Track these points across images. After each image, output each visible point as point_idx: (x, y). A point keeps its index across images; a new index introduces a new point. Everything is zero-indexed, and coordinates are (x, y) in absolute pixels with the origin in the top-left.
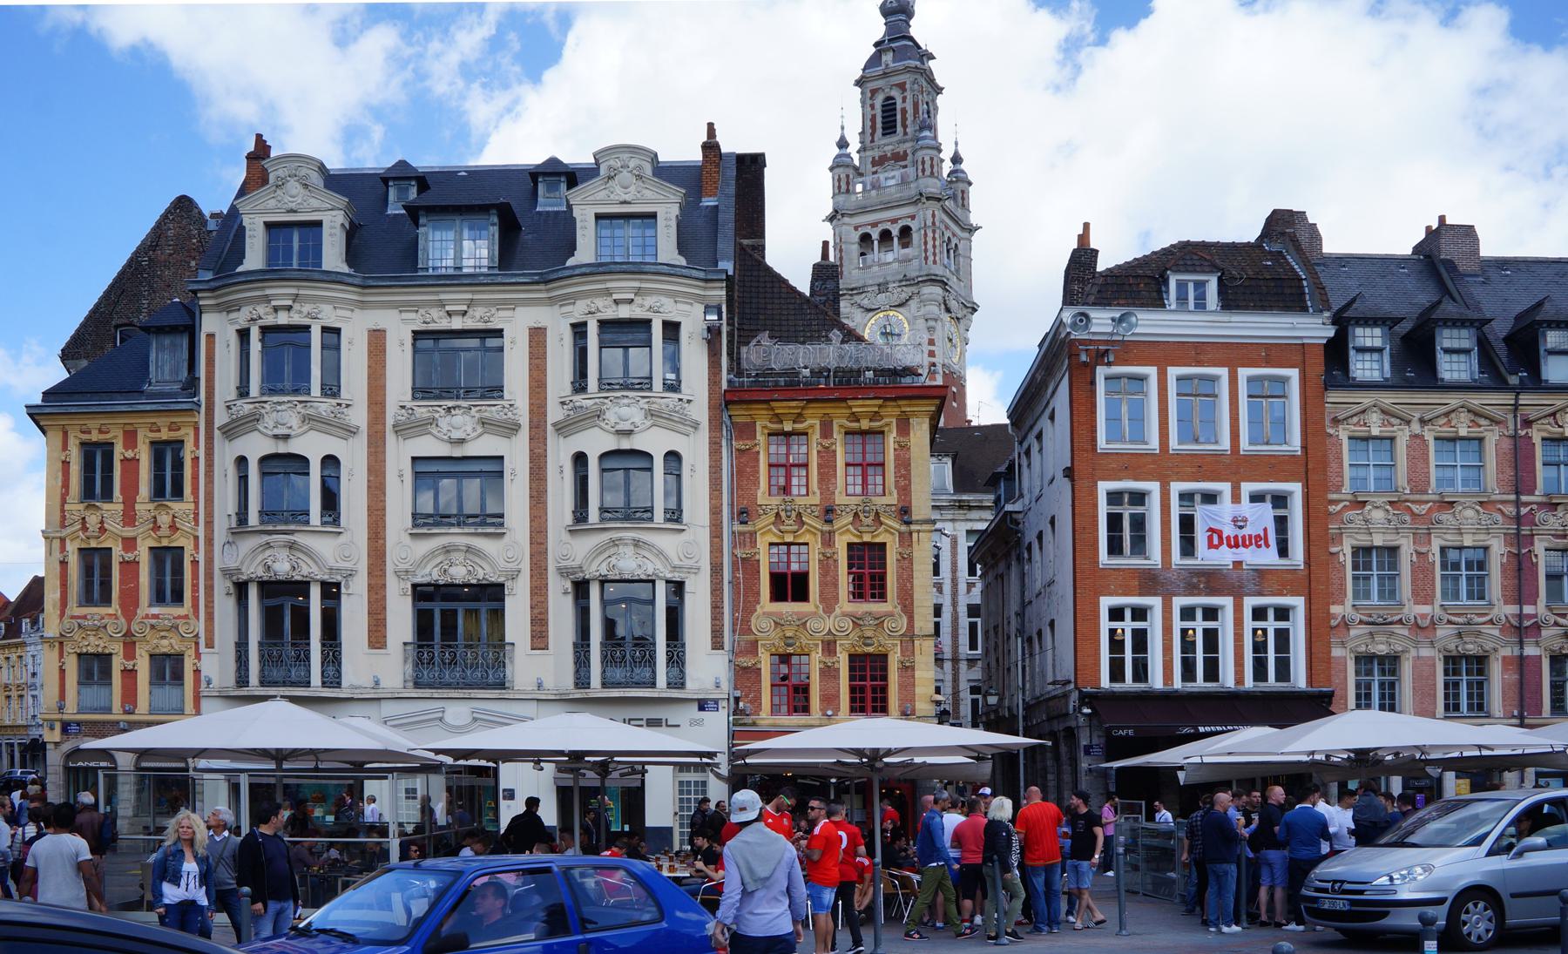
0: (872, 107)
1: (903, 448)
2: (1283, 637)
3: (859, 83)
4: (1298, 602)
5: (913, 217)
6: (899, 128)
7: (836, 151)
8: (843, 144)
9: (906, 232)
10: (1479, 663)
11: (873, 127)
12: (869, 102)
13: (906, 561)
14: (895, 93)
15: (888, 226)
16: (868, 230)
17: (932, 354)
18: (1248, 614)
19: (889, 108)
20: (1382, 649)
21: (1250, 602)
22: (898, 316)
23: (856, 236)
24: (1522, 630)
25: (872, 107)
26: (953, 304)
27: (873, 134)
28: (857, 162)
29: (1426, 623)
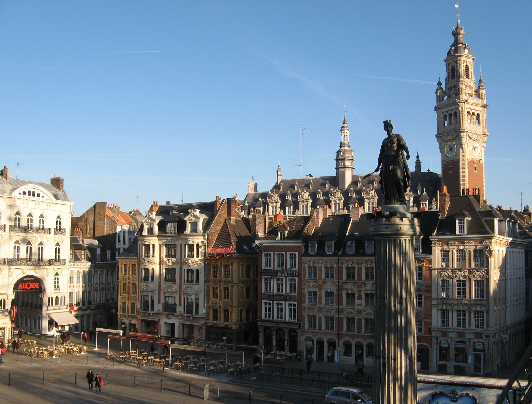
0: (449, 69)
1: (232, 268)
2: (295, 310)
3: (445, 61)
4: (296, 303)
5: (457, 109)
6: (456, 77)
8: (439, 84)
9: (455, 113)
10: (332, 318)
11: (449, 76)
13: (232, 291)
14: (454, 64)
15: (450, 112)
16: (445, 113)
17: (463, 156)
20: (311, 314)
21: (287, 303)
22: (453, 143)
23: (442, 116)
24: (339, 311)
25: (449, 69)
28: (444, 89)
29: (320, 309)
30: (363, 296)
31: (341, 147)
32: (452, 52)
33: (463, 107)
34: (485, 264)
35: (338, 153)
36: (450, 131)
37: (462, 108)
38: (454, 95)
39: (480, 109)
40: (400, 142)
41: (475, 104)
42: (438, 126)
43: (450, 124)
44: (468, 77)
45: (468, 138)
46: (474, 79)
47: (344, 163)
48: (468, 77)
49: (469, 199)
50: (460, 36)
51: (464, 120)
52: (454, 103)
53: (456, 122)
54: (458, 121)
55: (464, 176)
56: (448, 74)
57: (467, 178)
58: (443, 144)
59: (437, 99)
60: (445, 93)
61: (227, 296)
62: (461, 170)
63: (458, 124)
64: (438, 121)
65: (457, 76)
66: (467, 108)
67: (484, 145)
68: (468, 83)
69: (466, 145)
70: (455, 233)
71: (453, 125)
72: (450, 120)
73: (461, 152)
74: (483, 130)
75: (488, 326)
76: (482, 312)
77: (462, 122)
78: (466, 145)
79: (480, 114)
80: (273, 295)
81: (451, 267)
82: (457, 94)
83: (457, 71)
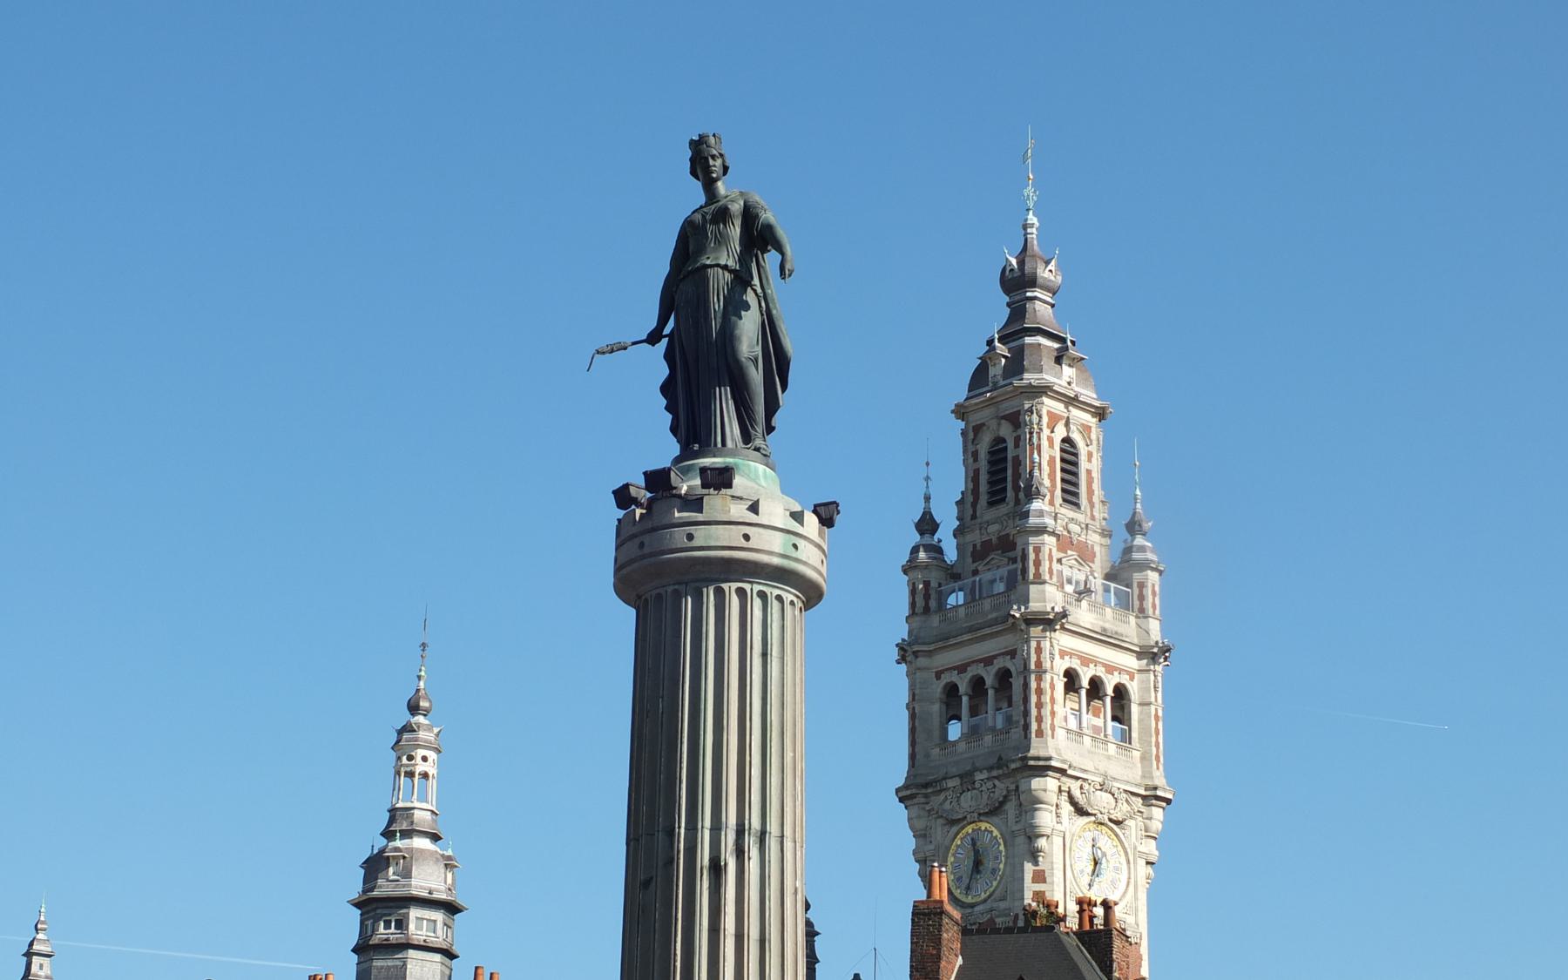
3: (960, 412)
5: (1012, 654)
6: (1010, 493)
7: (916, 538)
8: (927, 525)
9: (1004, 677)
11: (975, 492)
12: (971, 448)
14: (1006, 430)
15: (979, 670)
16: (953, 677)
19: (998, 455)
23: (938, 688)
25: (975, 455)
26: (1101, 802)
27: (974, 504)
28: (951, 554)
31: (388, 834)
32: (996, 371)
33: (1046, 645)
35: (375, 865)
36: (975, 769)
37: (1039, 650)
38: (1000, 587)
39: (1131, 662)
40: (757, 216)
42: (913, 743)
43: (972, 733)
44: (1071, 496)
45: (1067, 808)
46: (1100, 512)
47: (401, 924)
48: (1071, 496)
49: (1058, 944)
50: (1038, 293)
51: (1046, 712)
52: (995, 622)
53: (1009, 720)
54: (1017, 713)
56: (974, 478)
58: (939, 832)
59: (913, 605)
60: (953, 574)
63: (1016, 733)
64: (913, 717)
65: (1017, 488)
66: (1063, 654)
67: (1150, 848)
68: (1074, 528)
69: (1057, 841)
71: (988, 739)
72: (974, 712)
73: (1028, 876)
74: (1147, 774)
77: (1040, 719)
78: (1057, 841)
79: (1133, 688)
82: (1019, 579)
83: (1018, 462)
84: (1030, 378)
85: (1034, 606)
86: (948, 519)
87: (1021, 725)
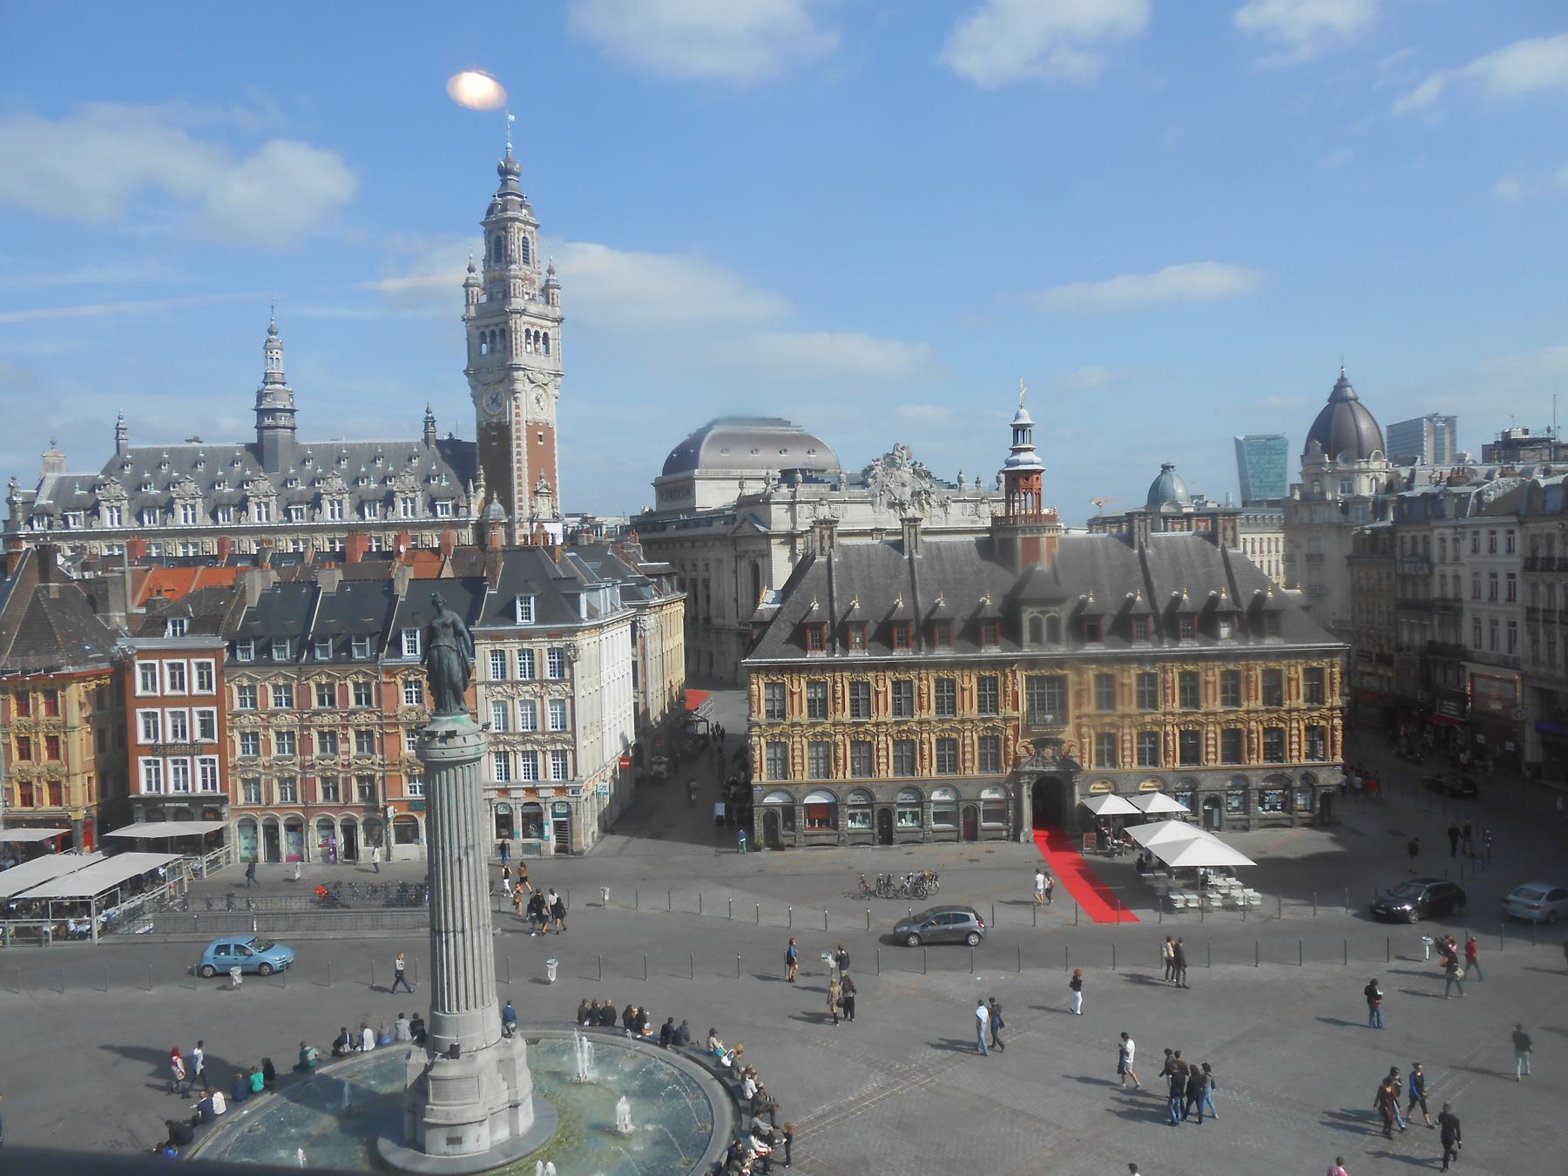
2: (213, 770)
4: (216, 757)
5: (506, 323)
9: (503, 331)
10: (292, 780)
17: (518, 415)
18: (197, 763)
23: (477, 333)
30: (352, 735)
34: (567, 676)
35: (261, 396)
39: (549, 324)
41: (540, 317)
43: (492, 350)
55: (519, 454)
56: (489, 251)
57: (525, 457)
61: (54, 753)
62: (514, 443)
70: (513, 618)
75: (575, 774)
76: (564, 752)
80: (165, 745)
81: (508, 677)
82: (506, 295)
84: (510, 214)
85: (513, 306)
86: (480, 267)
87: (507, 349)
